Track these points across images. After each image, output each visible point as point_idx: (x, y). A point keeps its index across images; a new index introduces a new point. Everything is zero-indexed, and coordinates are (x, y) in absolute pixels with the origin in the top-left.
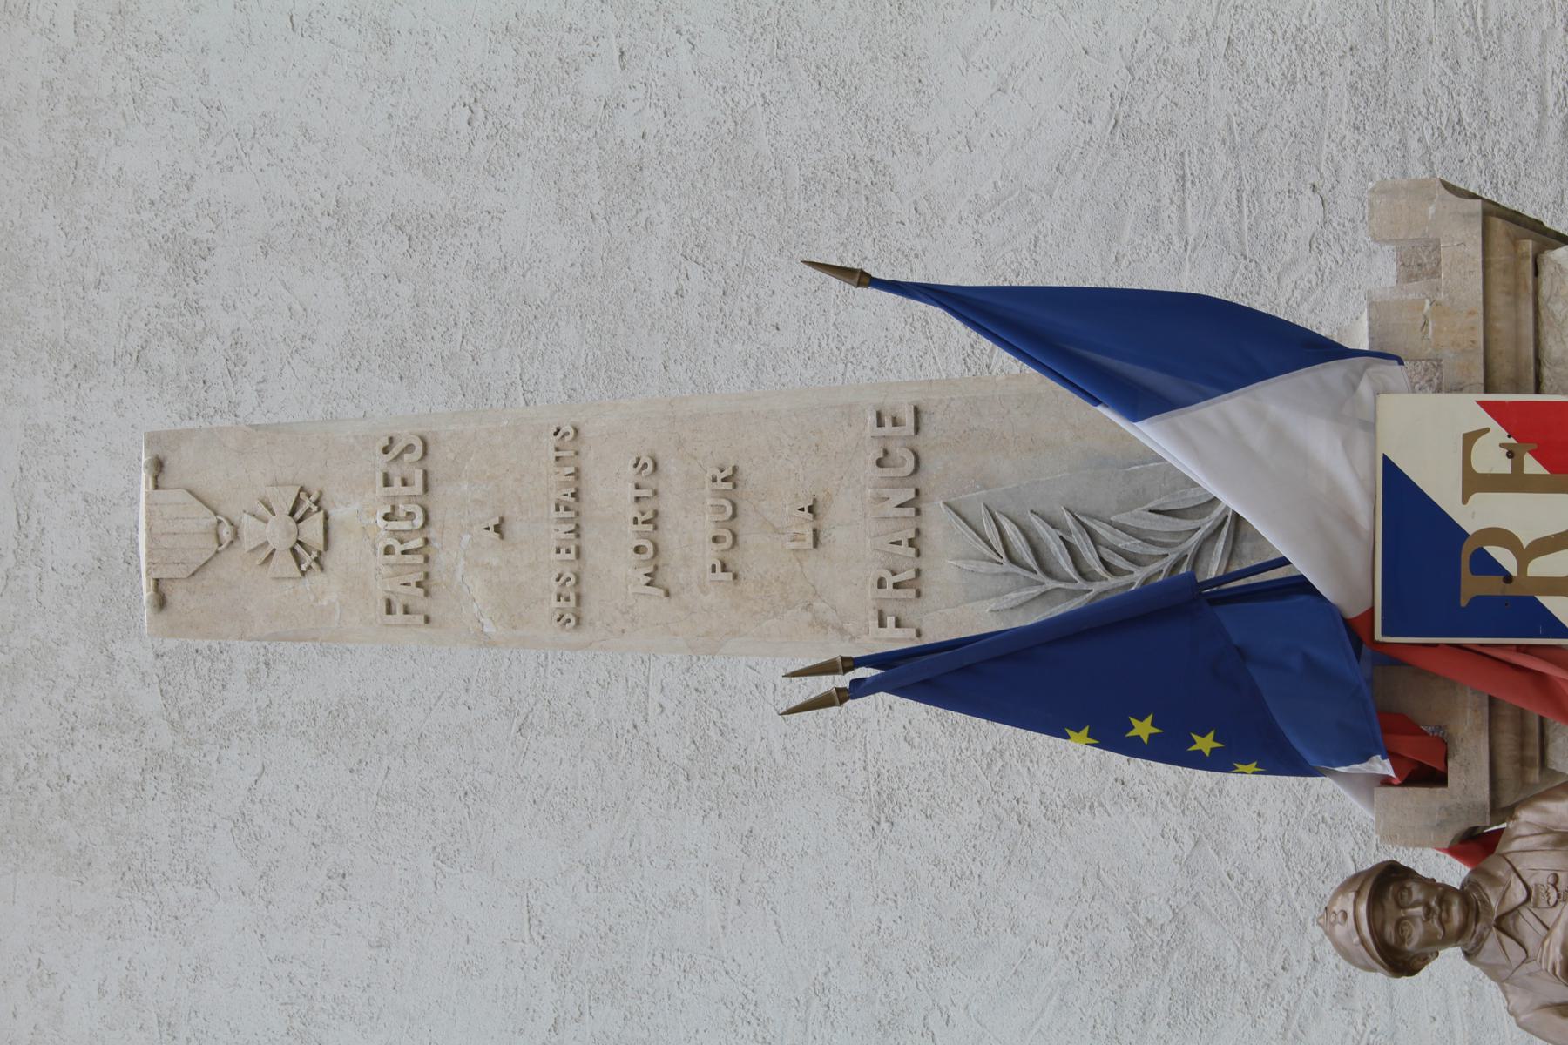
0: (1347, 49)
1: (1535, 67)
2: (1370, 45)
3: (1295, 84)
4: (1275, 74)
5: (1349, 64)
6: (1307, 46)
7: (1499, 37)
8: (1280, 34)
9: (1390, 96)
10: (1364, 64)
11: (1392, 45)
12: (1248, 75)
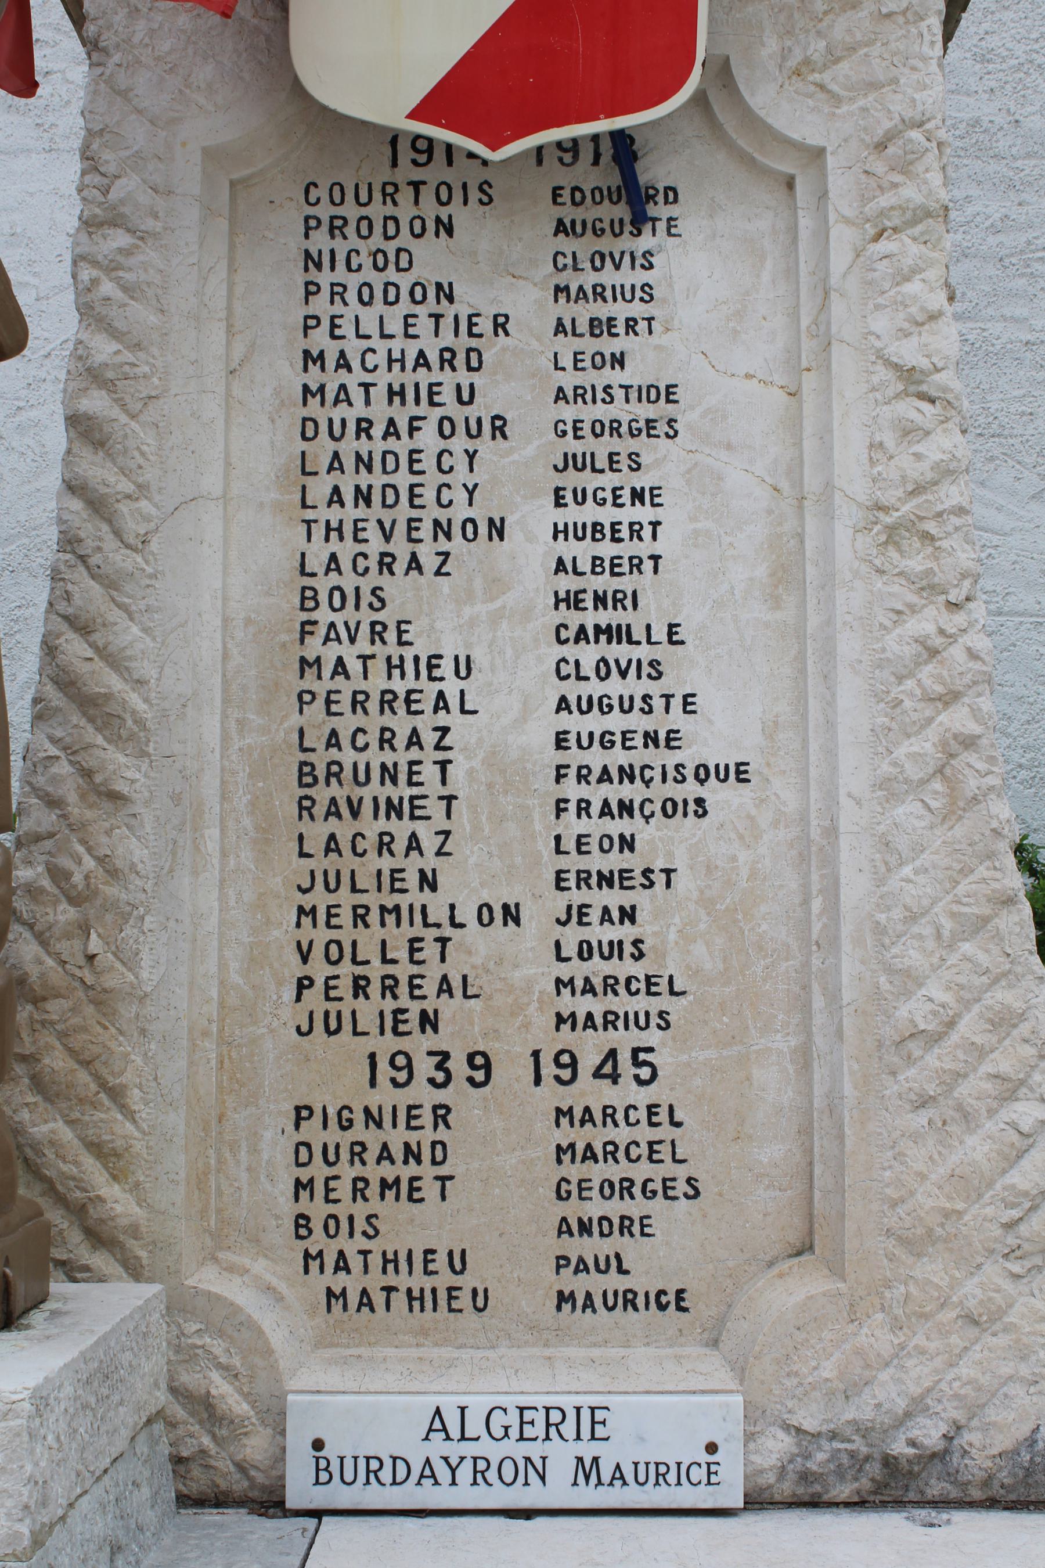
0: (1017, 117)
1: (990, 311)
2: (1019, 141)
3: (982, 62)
4: (993, 42)
5: (999, 120)
6: (1022, 75)
7: (1023, 275)
8: (1036, 47)
9: (965, 162)
10: (1000, 134)
11: (1019, 164)
12: (993, 13)
